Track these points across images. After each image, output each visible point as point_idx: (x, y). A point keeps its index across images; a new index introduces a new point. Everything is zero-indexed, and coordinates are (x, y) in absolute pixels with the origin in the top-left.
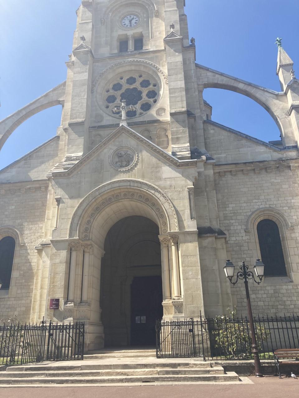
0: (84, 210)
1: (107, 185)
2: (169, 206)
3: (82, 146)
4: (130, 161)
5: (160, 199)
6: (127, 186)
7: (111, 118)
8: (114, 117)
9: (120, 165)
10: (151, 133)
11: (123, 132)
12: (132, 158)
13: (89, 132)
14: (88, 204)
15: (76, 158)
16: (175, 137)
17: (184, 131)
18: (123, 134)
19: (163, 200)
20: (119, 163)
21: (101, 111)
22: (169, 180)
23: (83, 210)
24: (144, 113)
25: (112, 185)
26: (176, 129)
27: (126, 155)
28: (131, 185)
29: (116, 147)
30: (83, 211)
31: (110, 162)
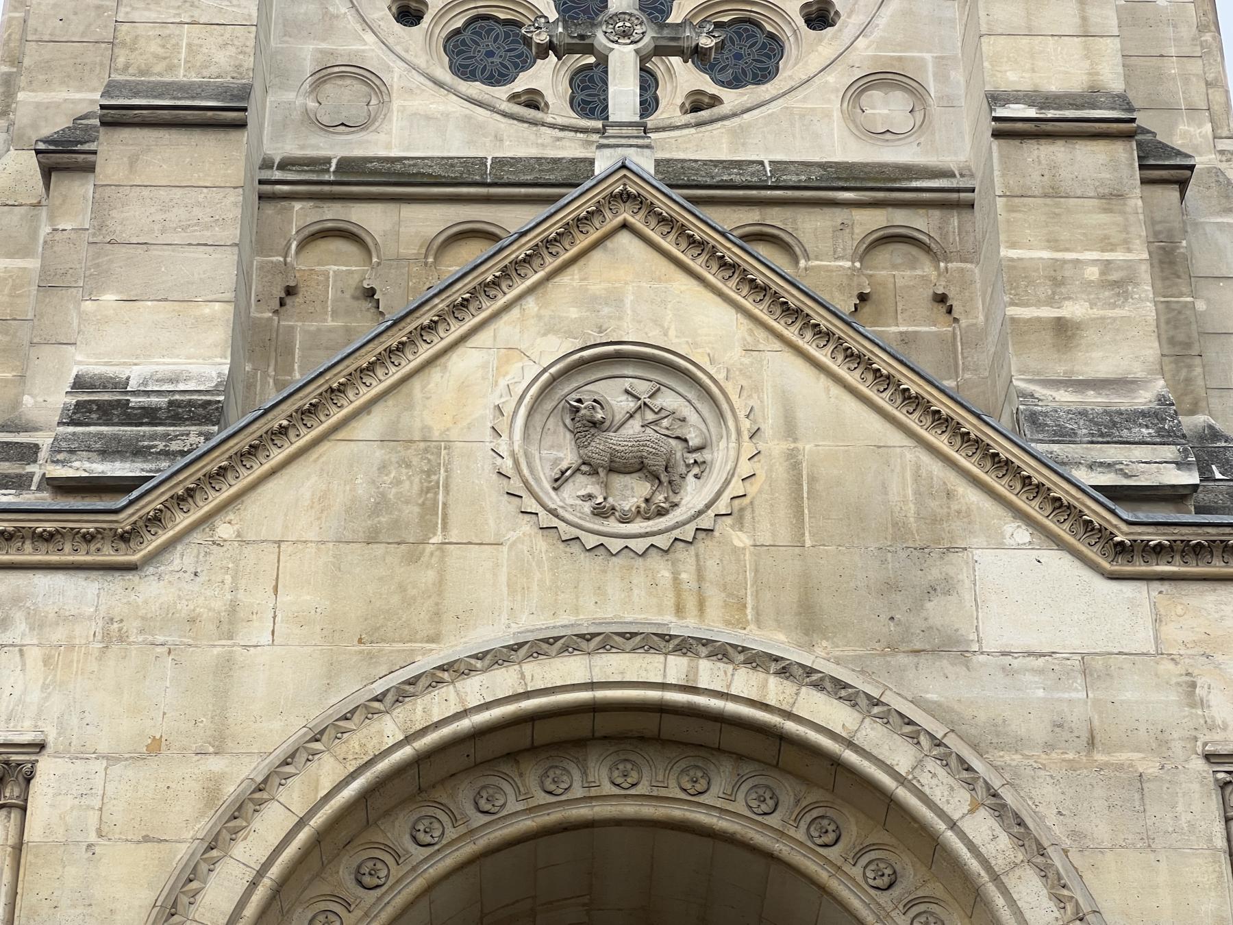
0: (261, 873)
1: (479, 664)
2: (1052, 905)
3: (217, 306)
4: (683, 477)
5: (967, 826)
6: (663, 686)
7: (455, 106)
8: (480, 104)
9: (590, 497)
10: (802, 263)
11: (625, 226)
12: (700, 449)
13: (262, 197)
14: (301, 823)
15: (171, 403)
16: (1039, 319)
17: (1115, 276)
18: (625, 238)
19: (995, 838)
20: (580, 478)
21: (369, 37)
22: (1034, 671)
23: (250, 875)
24: (731, 98)
25: (530, 668)
26: (1046, 254)
27: (650, 416)
28: (702, 684)
29: (569, 346)
30: (254, 884)
31: (509, 462)
